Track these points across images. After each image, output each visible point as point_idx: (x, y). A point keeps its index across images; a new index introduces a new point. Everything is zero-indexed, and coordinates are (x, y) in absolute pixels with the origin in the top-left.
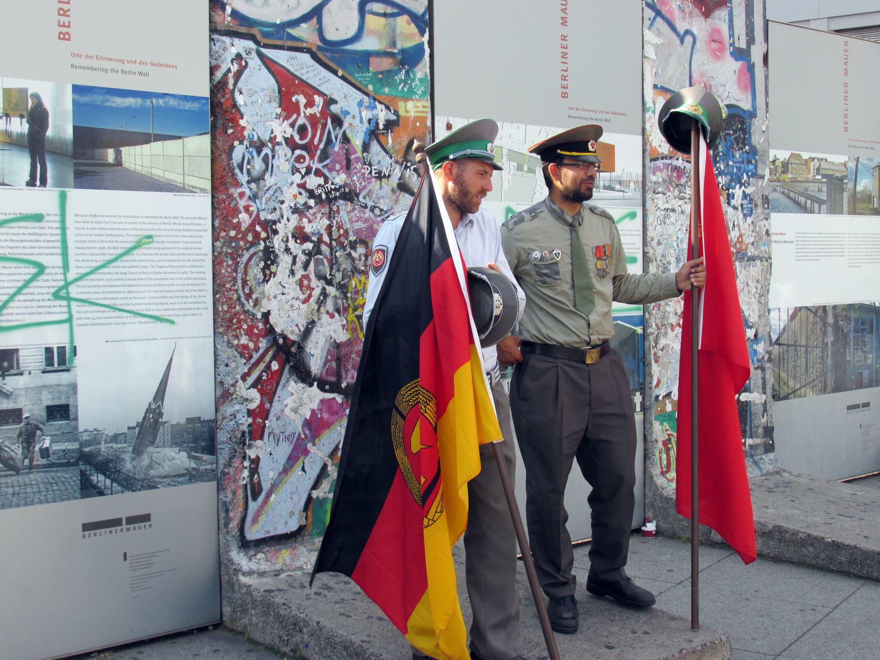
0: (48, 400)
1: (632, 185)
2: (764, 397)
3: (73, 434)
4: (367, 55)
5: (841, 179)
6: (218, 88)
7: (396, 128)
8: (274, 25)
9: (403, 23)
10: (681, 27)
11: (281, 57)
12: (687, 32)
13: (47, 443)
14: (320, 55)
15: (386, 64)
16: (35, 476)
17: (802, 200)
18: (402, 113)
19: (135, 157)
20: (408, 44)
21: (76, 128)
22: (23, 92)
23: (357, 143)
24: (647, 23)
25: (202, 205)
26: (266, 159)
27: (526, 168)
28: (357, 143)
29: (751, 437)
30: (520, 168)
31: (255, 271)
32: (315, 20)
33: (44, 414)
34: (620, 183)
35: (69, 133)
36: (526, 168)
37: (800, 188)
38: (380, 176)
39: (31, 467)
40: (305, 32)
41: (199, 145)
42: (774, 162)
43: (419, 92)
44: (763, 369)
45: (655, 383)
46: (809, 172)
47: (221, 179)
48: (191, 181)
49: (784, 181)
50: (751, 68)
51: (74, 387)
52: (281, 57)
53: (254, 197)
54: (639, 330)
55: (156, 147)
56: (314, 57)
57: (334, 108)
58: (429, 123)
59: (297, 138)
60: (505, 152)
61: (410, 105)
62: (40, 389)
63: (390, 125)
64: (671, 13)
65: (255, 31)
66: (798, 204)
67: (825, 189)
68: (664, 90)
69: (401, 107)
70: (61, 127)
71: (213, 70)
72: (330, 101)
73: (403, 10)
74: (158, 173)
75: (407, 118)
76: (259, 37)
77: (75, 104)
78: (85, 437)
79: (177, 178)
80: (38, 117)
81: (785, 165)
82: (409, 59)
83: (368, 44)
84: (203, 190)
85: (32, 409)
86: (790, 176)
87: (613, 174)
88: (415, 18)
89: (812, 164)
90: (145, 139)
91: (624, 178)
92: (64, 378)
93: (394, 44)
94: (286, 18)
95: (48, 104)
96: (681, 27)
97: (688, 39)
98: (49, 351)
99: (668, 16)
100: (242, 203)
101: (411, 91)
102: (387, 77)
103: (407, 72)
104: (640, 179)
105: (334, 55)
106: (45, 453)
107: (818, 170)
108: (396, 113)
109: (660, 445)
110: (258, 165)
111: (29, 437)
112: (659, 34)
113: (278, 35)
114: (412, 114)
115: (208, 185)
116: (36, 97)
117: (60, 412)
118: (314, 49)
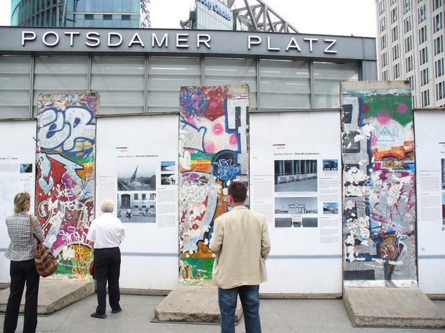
9: (87, 143)
10: (198, 126)
11: (52, 156)
12: (202, 127)
15: (81, 154)
18: (85, 166)
40: (58, 149)
50: (239, 135)
52: (52, 156)
64: (194, 122)
69: (85, 165)
73: (87, 139)
82: (89, 151)
83: (76, 149)
96: (198, 126)
97: (203, 130)
99: (193, 124)
105: (67, 154)
109: (183, 268)
112: (187, 130)
113: (52, 151)
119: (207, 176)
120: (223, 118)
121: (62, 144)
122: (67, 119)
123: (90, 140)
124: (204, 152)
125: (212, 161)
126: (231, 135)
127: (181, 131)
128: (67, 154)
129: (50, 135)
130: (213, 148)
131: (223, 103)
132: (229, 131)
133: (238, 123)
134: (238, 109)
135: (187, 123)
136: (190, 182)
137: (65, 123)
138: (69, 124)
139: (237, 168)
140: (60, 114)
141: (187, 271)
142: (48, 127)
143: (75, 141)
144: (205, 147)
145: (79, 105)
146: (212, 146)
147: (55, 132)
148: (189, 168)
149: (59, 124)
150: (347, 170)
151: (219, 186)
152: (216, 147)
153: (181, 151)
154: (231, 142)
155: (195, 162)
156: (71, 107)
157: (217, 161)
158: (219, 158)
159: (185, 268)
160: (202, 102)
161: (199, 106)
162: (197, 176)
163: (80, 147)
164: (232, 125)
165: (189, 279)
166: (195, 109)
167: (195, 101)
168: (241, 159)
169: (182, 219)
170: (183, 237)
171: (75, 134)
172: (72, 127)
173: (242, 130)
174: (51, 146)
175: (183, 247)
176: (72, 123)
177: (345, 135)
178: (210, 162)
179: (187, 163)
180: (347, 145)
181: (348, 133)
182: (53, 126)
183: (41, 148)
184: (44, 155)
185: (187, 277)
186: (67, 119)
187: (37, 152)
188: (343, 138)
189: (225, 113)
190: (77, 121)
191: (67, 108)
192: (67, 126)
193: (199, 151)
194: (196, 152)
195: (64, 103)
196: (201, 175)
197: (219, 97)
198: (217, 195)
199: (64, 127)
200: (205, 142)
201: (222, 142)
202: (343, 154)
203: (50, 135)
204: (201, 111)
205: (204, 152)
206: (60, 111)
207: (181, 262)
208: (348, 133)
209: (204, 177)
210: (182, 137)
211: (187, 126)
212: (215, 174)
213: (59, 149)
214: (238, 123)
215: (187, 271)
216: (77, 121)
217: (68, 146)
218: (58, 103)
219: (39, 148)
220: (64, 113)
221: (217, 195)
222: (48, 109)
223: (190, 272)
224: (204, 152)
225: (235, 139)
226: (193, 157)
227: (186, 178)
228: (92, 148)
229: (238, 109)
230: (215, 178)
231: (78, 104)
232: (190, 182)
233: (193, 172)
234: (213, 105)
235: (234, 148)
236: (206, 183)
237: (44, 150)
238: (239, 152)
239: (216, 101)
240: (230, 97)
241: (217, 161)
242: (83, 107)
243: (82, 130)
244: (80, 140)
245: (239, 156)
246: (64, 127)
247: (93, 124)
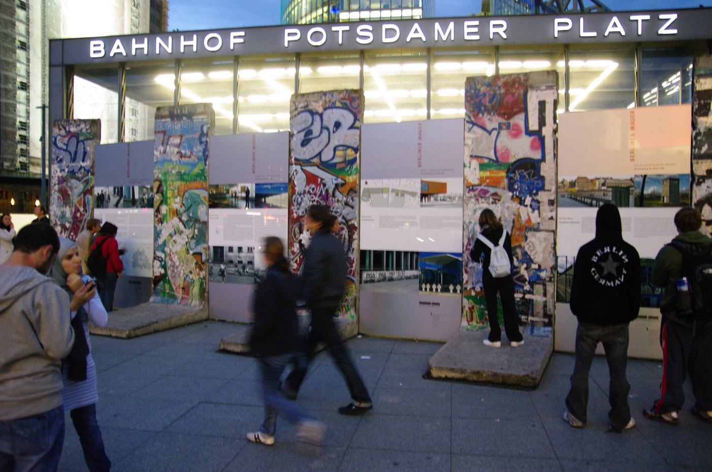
0: (248, 259)
1: (457, 199)
2: (544, 299)
3: (253, 269)
4: (335, 164)
5: (628, 188)
6: (290, 180)
7: (345, 186)
8: (307, 160)
9: (350, 152)
13: (247, 270)
14: (320, 166)
15: (344, 165)
16: (244, 278)
17: (589, 201)
18: (347, 180)
19: (269, 200)
20: (351, 158)
21: (256, 195)
22: (245, 187)
23: (331, 191)
24: (467, 129)
25: (287, 211)
26: (302, 199)
27: (400, 195)
28: (331, 191)
29: (533, 315)
30: (397, 195)
31: (297, 230)
32: (319, 156)
33: (247, 263)
34: (450, 198)
35: (254, 195)
36: (400, 195)
37: (587, 194)
38: (338, 201)
39: (244, 275)
41: (285, 196)
42: (562, 183)
43: (354, 173)
44: (544, 285)
45: (464, 282)
46: (595, 185)
47: (290, 204)
48: (283, 205)
49: (572, 192)
50: (542, 140)
51: (254, 257)
53: (298, 209)
54: (460, 259)
55: (274, 197)
56: (318, 167)
57: (323, 181)
58: (358, 182)
59: (311, 191)
60: (390, 190)
61: (350, 178)
62: (246, 257)
63: (343, 185)
64: (484, 123)
65: (301, 163)
66: (581, 201)
67: (610, 194)
68: (476, 157)
70: (253, 194)
71: (289, 174)
72: (322, 179)
73: (349, 147)
74: (275, 204)
75: (349, 182)
76: (302, 164)
77: (256, 188)
78: (256, 270)
79: (279, 205)
80: (248, 192)
81: (573, 184)
83: (336, 160)
84: (286, 208)
85: (245, 262)
86: (577, 188)
87: (446, 195)
88: (353, 149)
89: (597, 182)
90: (272, 195)
91: (452, 195)
92: (252, 255)
93: (345, 159)
94: (310, 157)
95: (250, 189)
98: (249, 248)
100: (294, 211)
101: (351, 173)
102: (342, 170)
103: (350, 168)
104: (462, 195)
105: (327, 166)
106: (247, 272)
107: (603, 185)
108: (345, 181)
109: (467, 309)
110: (300, 200)
111: (244, 268)
112: (475, 133)
113: (308, 162)
114: (351, 180)
115: (287, 206)
116: (248, 188)
117: (251, 263)
118: (318, 164)
119: (500, 191)
120: (522, 116)
121: (320, 154)
122: (325, 123)
123: (353, 149)
124: (497, 161)
125: (507, 173)
126: (532, 138)
127: (467, 135)
128: (327, 166)
129: (305, 143)
130: (508, 155)
131: (522, 97)
132: (529, 133)
133: (542, 122)
134: (542, 104)
135: (474, 124)
136: (477, 200)
137: (322, 128)
138: (327, 129)
139: (540, 182)
140: (317, 118)
141: (472, 313)
142: (303, 134)
143: (335, 150)
144: (498, 154)
145: (341, 105)
146: (507, 152)
147: (311, 139)
148: (476, 182)
149: (316, 129)
150: (699, 184)
151: (515, 205)
152: (513, 153)
153: (467, 160)
154: (533, 147)
155: (488, 174)
156: (329, 108)
157: (514, 172)
158: (518, 168)
159: (469, 309)
160: (494, 95)
161: (491, 101)
162: (487, 192)
163: (340, 157)
164: (534, 125)
165: (474, 323)
166: (485, 107)
167: (484, 95)
168: (546, 170)
169: (466, 246)
170: (469, 270)
171: (335, 142)
172: (331, 132)
173: (547, 131)
174: (307, 157)
175: (467, 282)
176: (331, 128)
177: (698, 134)
178: (503, 174)
179: (474, 174)
180: (700, 149)
181: (702, 130)
182: (309, 132)
183: (296, 159)
184: (298, 168)
185: (472, 319)
186: (325, 123)
187: (290, 164)
188: (695, 138)
189: (525, 110)
190: (338, 125)
191: (325, 109)
192: (325, 132)
193: (490, 159)
194: (486, 161)
195: (321, 103)
196: (492, 190)
197: (518, 89)
198: (513, 217)
199: (321, 132)
200: (499, 147)
201: (521, 148)
202: (694, 161)
203: (305, 143)
204: (493, 108)
205: (496, 162)
206: (317, 113)
207: (465, 301)
208: (702, 130)
209: (495, 194)
210: (469, 142)
211: (475, 128)
212: (511, 188)
213: (316, 160)
214: (542, 122)
215: (472, 313)
216: (338, 125)
217: (326, 157)
218: (314, 104)
219: (293, 159)
220: (321, 115)
221: (513, 217)
222: (302, 112)
223: (476, 314)
224: (497, 161)
225: (538, 143)
226: (483, 167)
227: (472, 194)
228: (355, 159)
229: (542, 104)
230: (511, 194)
231: (338, 104)
232: (477, 200)
233: (482, 187)
234: (509, 99)
235: (537, 155)
236: (499, 200)
237: (298, 161)
238: (543, 159)
239: (513, 94)
240: (532, 87)
241: (514, 172)
242: (345, 107)
243: (343, 136)
244: (341, 148)
245: (543, 165)
246: (321, 132)
247: (357, 128)
